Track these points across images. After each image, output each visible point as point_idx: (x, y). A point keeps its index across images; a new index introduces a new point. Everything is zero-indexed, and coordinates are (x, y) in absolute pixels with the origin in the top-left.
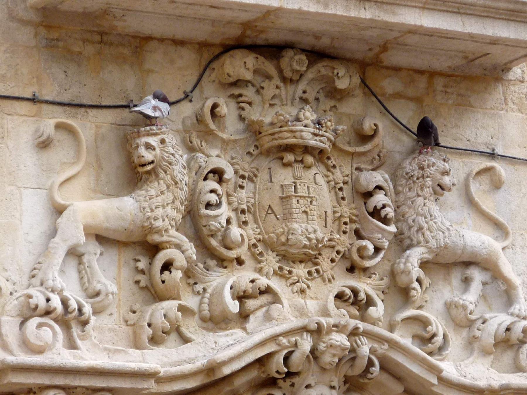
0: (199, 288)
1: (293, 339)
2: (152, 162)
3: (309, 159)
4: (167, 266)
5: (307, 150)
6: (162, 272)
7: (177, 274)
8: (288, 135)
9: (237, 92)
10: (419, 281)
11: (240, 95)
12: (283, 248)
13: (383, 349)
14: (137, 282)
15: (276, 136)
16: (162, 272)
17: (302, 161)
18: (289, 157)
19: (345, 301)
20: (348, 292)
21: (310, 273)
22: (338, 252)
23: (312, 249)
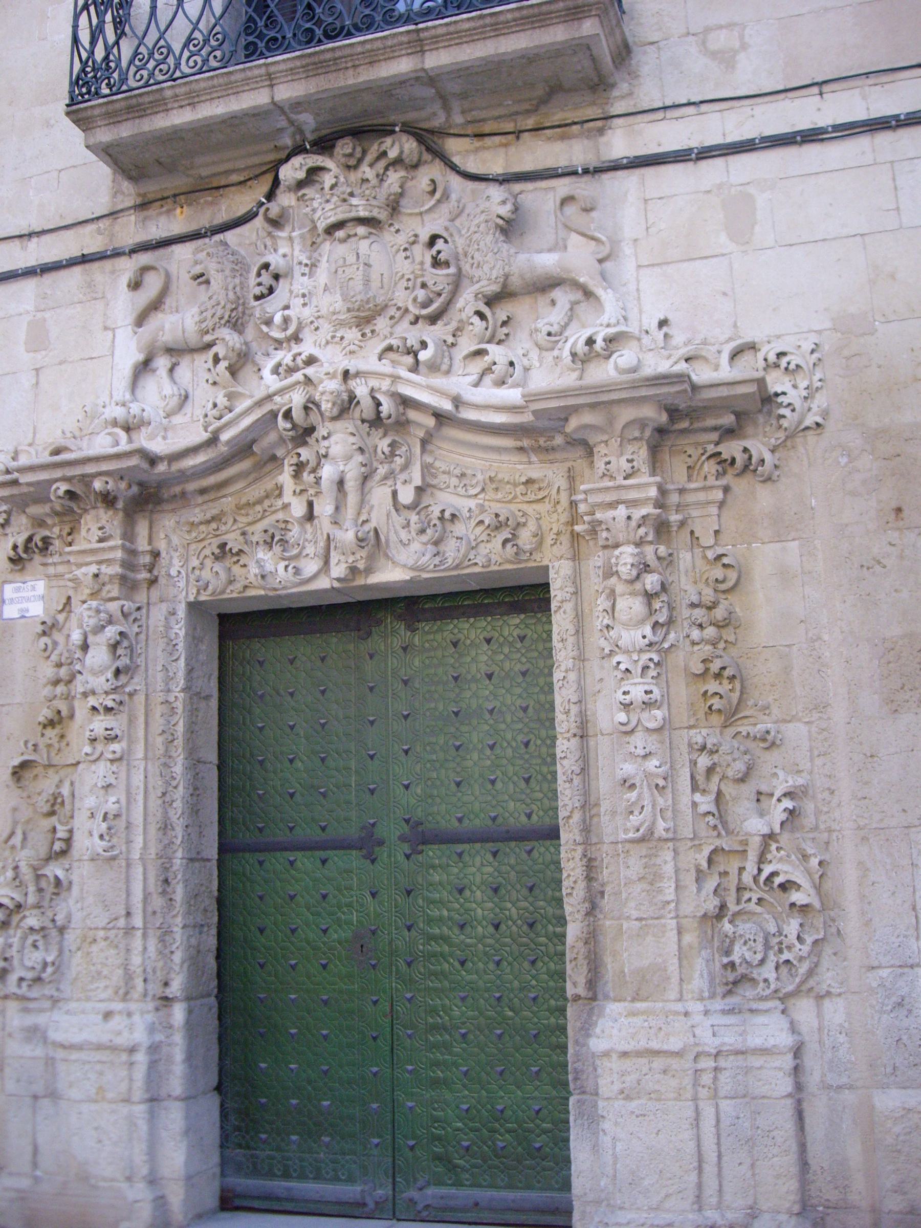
1: (287, 396)
3: (361, 230)
4: (216, 360)
7: (223, 365)
8: (332, 213)
11: (304, 195)
12: (334, 317)
17: (356, 235)
18: (340, 234)
21: (363, 335)
23: (358, 310)
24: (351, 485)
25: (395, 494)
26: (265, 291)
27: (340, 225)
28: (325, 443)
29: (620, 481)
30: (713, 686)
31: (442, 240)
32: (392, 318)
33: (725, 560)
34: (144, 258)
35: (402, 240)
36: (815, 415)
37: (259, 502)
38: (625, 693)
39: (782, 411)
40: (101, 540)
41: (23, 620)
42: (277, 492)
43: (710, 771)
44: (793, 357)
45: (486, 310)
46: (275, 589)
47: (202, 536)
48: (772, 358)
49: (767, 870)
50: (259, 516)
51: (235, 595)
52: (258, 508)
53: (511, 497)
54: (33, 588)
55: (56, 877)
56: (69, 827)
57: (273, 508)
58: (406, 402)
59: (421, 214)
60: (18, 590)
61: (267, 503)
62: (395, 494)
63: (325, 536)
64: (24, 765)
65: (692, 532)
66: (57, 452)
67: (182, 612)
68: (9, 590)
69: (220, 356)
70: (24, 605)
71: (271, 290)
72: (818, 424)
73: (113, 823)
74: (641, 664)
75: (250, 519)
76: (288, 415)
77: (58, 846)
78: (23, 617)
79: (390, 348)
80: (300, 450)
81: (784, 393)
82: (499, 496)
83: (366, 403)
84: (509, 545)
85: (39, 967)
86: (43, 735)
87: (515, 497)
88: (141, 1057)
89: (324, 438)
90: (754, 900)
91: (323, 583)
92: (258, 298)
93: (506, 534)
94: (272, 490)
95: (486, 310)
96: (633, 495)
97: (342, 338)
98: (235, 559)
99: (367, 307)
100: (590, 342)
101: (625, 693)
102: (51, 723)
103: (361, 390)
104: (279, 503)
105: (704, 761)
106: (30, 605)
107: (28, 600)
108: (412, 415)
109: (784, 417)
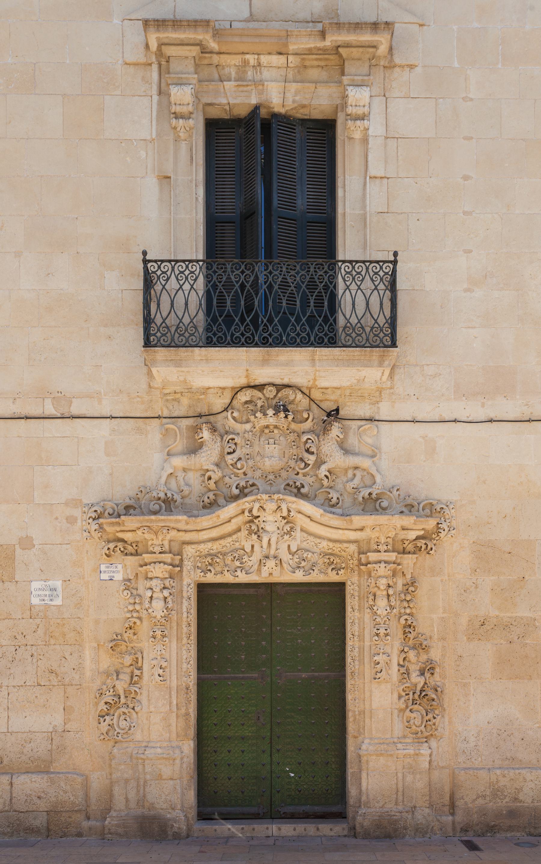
10: (327, 477)
22: (291, 468)
31: (311, 441)
39: (440, 531)
41: (110, 581)
49: (424, 694)
54: (116, 567)
55: (135, 691)
60: (108, 567)
68: (103, 568)
70: (112, 574)
71: (234, 451)
79: (288, 485)
85: (127, 728)
86: (126, 632)
88: (178, 761)
90: (418, 703)
100: (370, 494)
107: (114, 572)
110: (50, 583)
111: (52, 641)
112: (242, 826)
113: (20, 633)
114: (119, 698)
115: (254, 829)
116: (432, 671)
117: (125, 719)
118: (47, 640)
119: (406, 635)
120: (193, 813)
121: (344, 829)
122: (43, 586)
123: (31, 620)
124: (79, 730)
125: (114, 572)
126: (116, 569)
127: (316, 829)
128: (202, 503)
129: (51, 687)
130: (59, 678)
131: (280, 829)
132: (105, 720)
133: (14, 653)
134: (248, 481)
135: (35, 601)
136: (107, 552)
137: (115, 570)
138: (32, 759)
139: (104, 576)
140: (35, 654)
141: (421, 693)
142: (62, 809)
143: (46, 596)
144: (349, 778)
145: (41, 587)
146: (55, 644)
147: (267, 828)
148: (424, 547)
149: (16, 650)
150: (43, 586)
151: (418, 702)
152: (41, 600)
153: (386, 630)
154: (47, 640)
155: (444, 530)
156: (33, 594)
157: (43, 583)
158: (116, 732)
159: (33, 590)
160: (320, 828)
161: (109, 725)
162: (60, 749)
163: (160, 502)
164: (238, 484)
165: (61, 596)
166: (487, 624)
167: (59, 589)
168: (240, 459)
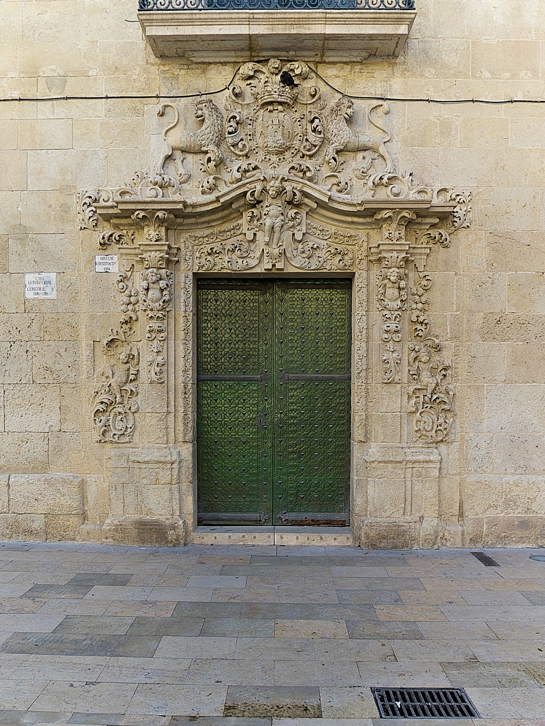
0: (229, 170)
1: (253, 185)
2: (202, 116)
3: (280, 108)
4: (209, 160)
5: (280, 103)
6: (208, 163)
7: (213, 163)
9: (249, 82)
10: (334, 158)
13: (299, 187)
14: (201, 169)
15: (262, 99)
16: (208, 163)
17: (277, 110)
18: (270, 108)
19: (296, 170)
20: (296, 166)
22: (296, 149)
24: (277, 229)
25: (294, 234)
26: (234, 131)
27: (271, 103)
28: (268, 209)
29: (394, 242)
30: (419, 327)
31: (318, 120)
32: (293, 153)
33: (428, 278)
34: (167, 102)
35: (297, 115)
36: (467, 222)
37: (229, 231)
38: (387, 326)
39: (455, 219)
40: (155, 241)
42: (238, 227)
43: (416, 359)
44: (462, 197)
45: (336, 156)
46: (236, 271)
47: (201, 243)
48: (454, 196)
49: (435, 397)
50: (229, 237)
51: (216, 271)
52: (228, 233)
53: (342, 241)
54: (112, 258)
55: (131, 390)
56: (137, 369)
57: (235, 235)
58: (305, 195)
59: (307, 104)
60: (103, 259)
61: (232, 232)
62: (294, 234)
63: (261, 250)
64: (112, 340)
65: (415, 265)
66: (122, 194)
67: (191, 277)
68: (98, 259)
69: (212, 159)
72: (468, 226)
73: (162, 368)
74: (394, 316)
75: (224, 238)
76: (252, 194)
77: (132, 377)
78: (107, 272)
79: (293, 168)
80: (253, 210)
81: (457, 212)
82: (337, 240)
83: (290, 194)
84: (341, 262)
86: (122, 327)
87: (344, 242)
88: (175, 466)
89: (267, 206)
90: (429, 407)
91: (258, 270)
92: (230, 133)
93: (339, 257)
94: (236, 226)
95: (336, 156)
96: (398, 248)
97: (270, 159)
98: (217, 255)
99: (283, 146)
100: (381, 178)
101: (387, 326)
102: (126, 322)
103: (288, 187)
104: (239, 232)
105: (413, 354)
106: (111, 267)
107: (110, 264)
108: (306, 201)
109: (456, 222)
110: (44, 275)
111: (47, 337)
112: (243, 534)
113: (14, 328)
114: (116, 398)
115: (255, 537)
116: (443, 372)
117: (121, 420)
118: (42, 336)
119: (417, 333)
120: (191, 520)
121: (348, 539)
122: (37, 279)
123: (25, 315)
124: (74, 431)
125: (110, 264)
126: (112, 261)
127: (319, 538)
128: (201, 189)
129: (46, 385)
130: (54, 376)
131: (282, 538)
132: (101, 420)
133: (9, 349)
134: (250, 164)
135: (30, 295)
136: (102, 241)
137: (110, 261)
138: (29, 460)
139: (100, 268)
140: (30, 350)
141: (432, 396)
142: (59, 513)
143: (40, 289)
144: (355, 486)
145: (35, 280)
146: (50, 340)
147: (269, 537)
148: (438, 237)
149: (11, 346)
150: (37, 279)
151: (429, 406)
152: (35, 294)
153: (397, 327)
154: (42, 336)
155: (460, 219)
156: (27, 287)
157: (37, 275)
158: (112, 434)
159: (27, 283)
160: (323, 537)
161: (105, 426)
162: (57, 450)
163: (157, 187)
164: (240, 168)
165: (55, 289)
166: (503, 322)
167: (54, 281)
168: (242, 140)
